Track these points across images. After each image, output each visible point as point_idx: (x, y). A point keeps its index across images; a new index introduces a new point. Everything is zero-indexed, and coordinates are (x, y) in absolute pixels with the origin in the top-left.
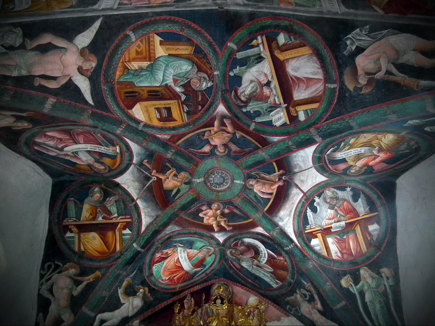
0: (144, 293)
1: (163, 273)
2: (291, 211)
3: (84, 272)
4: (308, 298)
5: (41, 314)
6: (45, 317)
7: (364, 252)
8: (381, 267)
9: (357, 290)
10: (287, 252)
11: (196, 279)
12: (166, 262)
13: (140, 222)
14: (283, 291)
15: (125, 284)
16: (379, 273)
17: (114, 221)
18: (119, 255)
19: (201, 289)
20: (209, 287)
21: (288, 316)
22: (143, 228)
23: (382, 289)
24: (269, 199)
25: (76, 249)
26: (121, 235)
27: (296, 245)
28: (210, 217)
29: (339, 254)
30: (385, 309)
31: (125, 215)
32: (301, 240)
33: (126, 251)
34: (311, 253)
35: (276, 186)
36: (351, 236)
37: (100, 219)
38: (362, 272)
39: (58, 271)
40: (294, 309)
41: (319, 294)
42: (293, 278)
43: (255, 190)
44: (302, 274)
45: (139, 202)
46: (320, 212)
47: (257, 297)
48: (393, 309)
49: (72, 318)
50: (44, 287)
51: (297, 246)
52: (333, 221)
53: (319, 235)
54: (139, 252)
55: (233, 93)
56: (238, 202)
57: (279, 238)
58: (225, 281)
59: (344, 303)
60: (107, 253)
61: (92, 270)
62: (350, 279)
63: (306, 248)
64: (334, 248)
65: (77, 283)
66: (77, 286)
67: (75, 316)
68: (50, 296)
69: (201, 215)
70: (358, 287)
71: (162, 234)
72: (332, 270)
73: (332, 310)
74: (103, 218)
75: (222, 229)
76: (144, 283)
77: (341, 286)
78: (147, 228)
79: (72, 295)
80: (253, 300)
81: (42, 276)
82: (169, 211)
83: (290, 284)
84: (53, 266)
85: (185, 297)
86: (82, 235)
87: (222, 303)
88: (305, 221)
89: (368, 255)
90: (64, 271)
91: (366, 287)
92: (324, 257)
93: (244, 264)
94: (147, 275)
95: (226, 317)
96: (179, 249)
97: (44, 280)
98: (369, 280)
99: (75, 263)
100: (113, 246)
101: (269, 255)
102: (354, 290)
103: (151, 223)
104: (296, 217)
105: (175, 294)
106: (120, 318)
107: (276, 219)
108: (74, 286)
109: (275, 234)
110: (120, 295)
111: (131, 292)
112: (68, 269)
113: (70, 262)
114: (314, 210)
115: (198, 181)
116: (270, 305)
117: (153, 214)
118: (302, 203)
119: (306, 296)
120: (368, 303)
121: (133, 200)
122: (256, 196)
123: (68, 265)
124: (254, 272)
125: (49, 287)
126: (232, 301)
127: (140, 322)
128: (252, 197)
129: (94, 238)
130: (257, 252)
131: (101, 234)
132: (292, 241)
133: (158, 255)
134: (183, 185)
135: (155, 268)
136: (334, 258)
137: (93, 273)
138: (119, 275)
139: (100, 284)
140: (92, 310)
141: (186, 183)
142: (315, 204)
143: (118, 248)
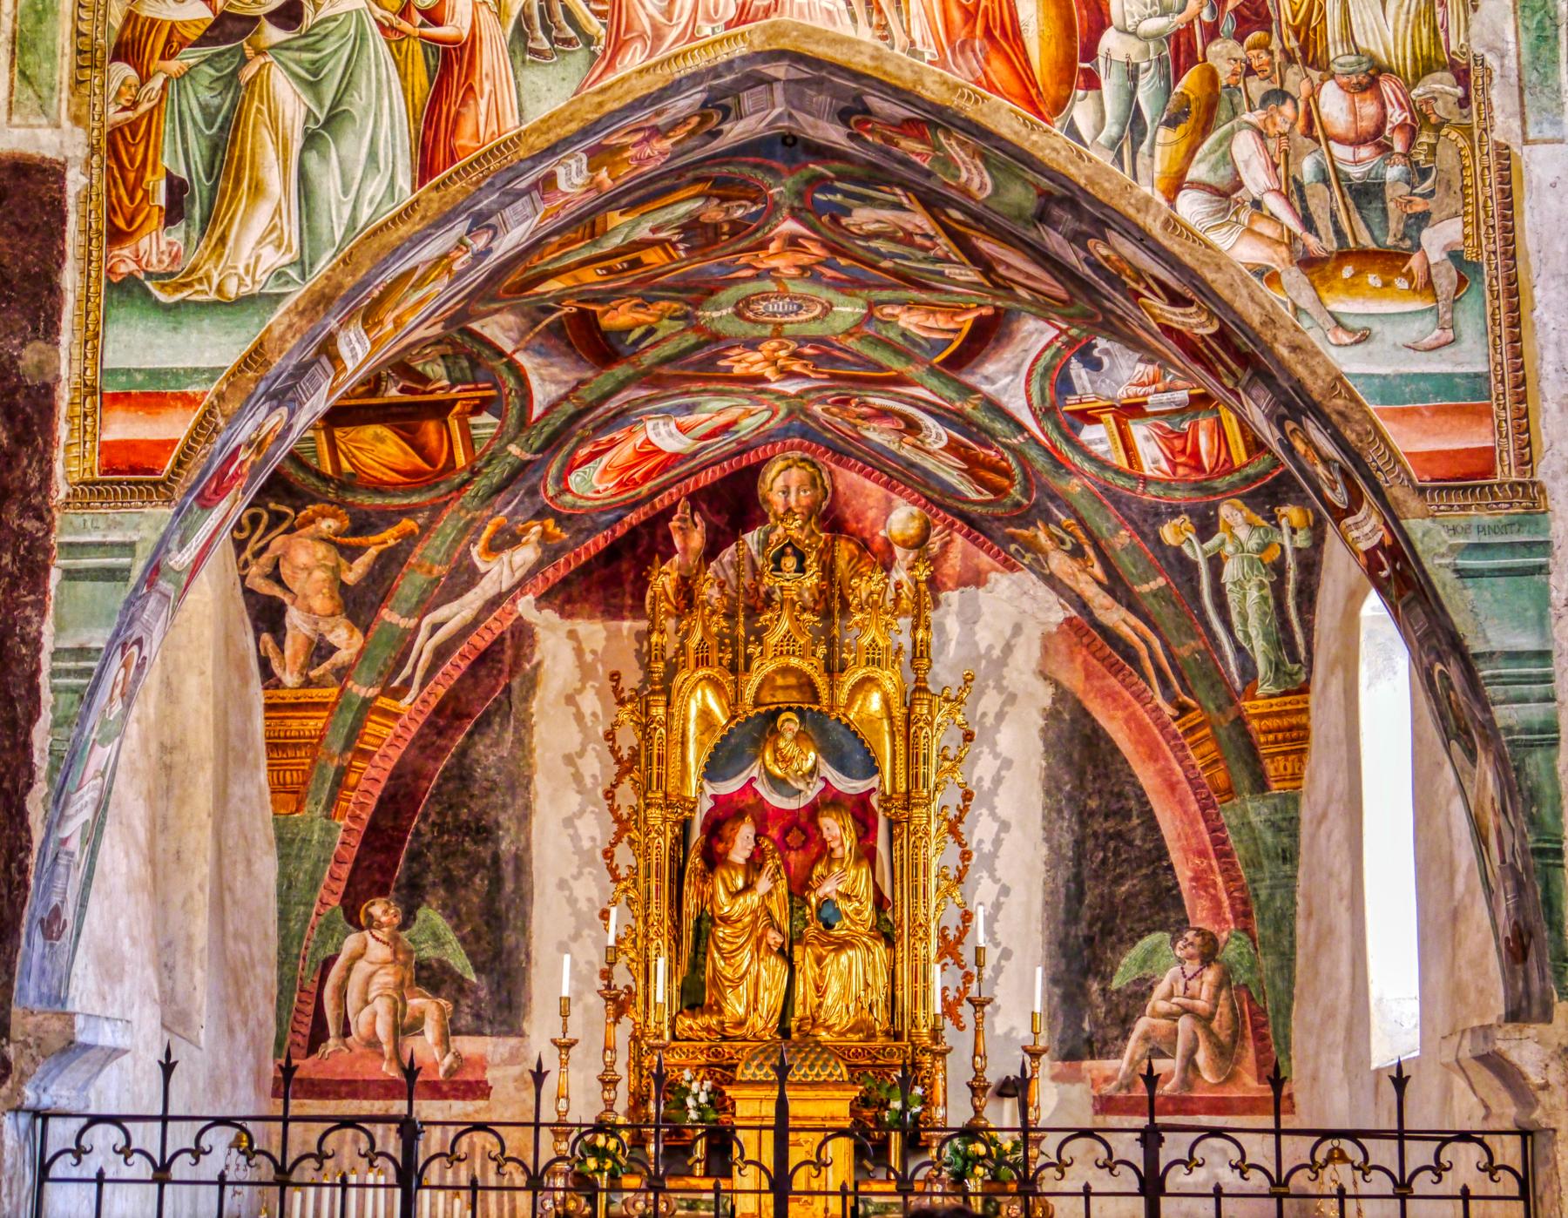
0: (544, 534)
1: (600, 481)
2: (1019, 366)
3: (363, 524)
4: (1068, 546)
5: (266, 637)
6: (280, 644)
7: (1237, 463)
8: (1282, 503)
9: (1205, 553)
10: (1006, 446)
11: (704, 457)
12: (606, 458)
13: (526, 396)
14: (999, 511)
15: (485, 535)
16: (1272, 518)
17: (439, 395)
18: (465, 475)
19: (723, 480)
20: (754, 472)
21: (1012, 568)
22: (537, 411)
23: (1275, 554)
24: (951, 342)
25: (328, 469)
26: (465, 430)
27: (1033, 437)
28: (753, 364)
29: (1164, 466)
30: (1271, 601)
31: (475, 382)
32: (1049, 427)
33: (488, 463)
34: (1077, 460)
35: (971, 316)
36: (1205, 423)
37: (393, 393)
38: (1224, 510)
39: (285, 526)
40: (1029, 556)
41: (1096, 545)
42: (1026, 492)
43: (902, 324)
44: (1053, 497)
45: (520, 358)
46: (1111, 369)
47: (915, 510)
48: (1291, 603)
49: (358, 639)
50: (254, 570)
51: (1037, 442)
52: (1152, 389)
53: (1108, 417)
54: (525, 464)
55: (825, 219)
56: (851, 343)
57: (982, 417)
58: (807, 450)
59: (1161, 581)
60: (425, 473)
61: (388, 518)
62: (1188, 524)
63: (1065, 448)
64: (1151, 453)
65: (351, 553)
66: (351, 560)
67: (366, 631)
68: (277, 592)
69: (722, 363)
70: (1208, 545)
71: (601, 410)
72: (1140, 502)
73: (1129, 591)
74: (402, 391)
75: (790, 375)
76: (540, 515)
77: (1159, 541)
78: (549, 410)
79: (343, 583)
80: (902, 519)
81: (240, 546)
82: (620, 371)
83: (1018, 505)
84: (266, 517)
85: (669, 512)
86: (338, 433)
87: (801, 569)
88: (1065, 385)
89: (1250, 471)
90: (302, 526)
91: (1229, 548)
92: (1118, 471)
93: (873, 436)
94: (551, 493)
95: (813, 611)
96: (650, 425)
97: (247, 554)
98: (1242, 533)
99: (332, 503)
100: (444, 457)
101: (950, 438)
102: (1197, 552)
103: (565, 398)
104: (1036, 378)
105: (635, 505)
106: (479, 604)
107: (971, 380)
108: (343, 561)
109: (968, 409)
110: (476, 559)
111: (506, 540)
112: (312, 521)
113: (314, 501)
114: (1095, 365)
115: (715, 314)
116: (956, 535)
117: (571, 377)
118: (1053, 350)
119: (1063, 542)
120: (1229, 586)
121: (500, 353)
122: (904, 335)
123: (310, 510)
124: (903, 453)
125: (268, 570)
126: (832, 519)
127: (538, 600)
128: (893, 334)
129: (380, 439)
130: (912, 427)
131: (402, 428)
132: (1021, 428)
133: (583, 452)
134: (666, 322)
135: (574, 480)
136: (1148, 473)
137: (391, 524)
138: (473, 520)
139: (417, 551)
140: (409, 615)
141: (671, 318)
142: (1096, 353)
143: (461, 459)
